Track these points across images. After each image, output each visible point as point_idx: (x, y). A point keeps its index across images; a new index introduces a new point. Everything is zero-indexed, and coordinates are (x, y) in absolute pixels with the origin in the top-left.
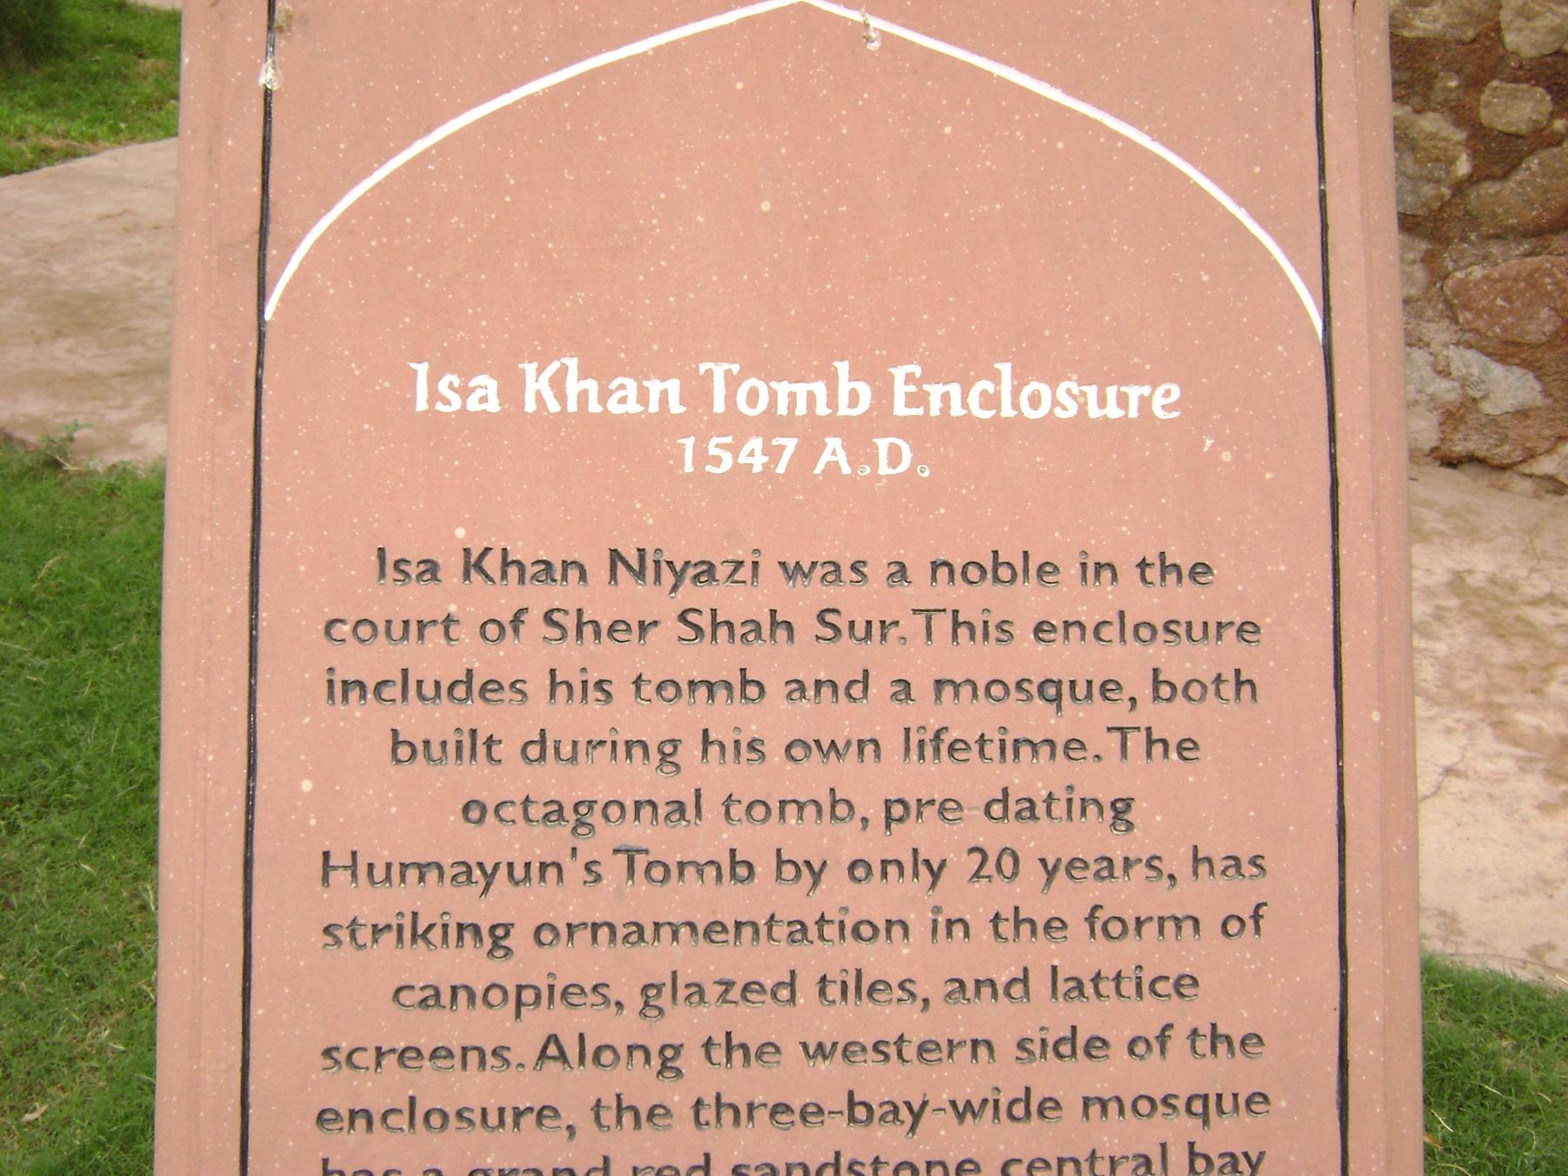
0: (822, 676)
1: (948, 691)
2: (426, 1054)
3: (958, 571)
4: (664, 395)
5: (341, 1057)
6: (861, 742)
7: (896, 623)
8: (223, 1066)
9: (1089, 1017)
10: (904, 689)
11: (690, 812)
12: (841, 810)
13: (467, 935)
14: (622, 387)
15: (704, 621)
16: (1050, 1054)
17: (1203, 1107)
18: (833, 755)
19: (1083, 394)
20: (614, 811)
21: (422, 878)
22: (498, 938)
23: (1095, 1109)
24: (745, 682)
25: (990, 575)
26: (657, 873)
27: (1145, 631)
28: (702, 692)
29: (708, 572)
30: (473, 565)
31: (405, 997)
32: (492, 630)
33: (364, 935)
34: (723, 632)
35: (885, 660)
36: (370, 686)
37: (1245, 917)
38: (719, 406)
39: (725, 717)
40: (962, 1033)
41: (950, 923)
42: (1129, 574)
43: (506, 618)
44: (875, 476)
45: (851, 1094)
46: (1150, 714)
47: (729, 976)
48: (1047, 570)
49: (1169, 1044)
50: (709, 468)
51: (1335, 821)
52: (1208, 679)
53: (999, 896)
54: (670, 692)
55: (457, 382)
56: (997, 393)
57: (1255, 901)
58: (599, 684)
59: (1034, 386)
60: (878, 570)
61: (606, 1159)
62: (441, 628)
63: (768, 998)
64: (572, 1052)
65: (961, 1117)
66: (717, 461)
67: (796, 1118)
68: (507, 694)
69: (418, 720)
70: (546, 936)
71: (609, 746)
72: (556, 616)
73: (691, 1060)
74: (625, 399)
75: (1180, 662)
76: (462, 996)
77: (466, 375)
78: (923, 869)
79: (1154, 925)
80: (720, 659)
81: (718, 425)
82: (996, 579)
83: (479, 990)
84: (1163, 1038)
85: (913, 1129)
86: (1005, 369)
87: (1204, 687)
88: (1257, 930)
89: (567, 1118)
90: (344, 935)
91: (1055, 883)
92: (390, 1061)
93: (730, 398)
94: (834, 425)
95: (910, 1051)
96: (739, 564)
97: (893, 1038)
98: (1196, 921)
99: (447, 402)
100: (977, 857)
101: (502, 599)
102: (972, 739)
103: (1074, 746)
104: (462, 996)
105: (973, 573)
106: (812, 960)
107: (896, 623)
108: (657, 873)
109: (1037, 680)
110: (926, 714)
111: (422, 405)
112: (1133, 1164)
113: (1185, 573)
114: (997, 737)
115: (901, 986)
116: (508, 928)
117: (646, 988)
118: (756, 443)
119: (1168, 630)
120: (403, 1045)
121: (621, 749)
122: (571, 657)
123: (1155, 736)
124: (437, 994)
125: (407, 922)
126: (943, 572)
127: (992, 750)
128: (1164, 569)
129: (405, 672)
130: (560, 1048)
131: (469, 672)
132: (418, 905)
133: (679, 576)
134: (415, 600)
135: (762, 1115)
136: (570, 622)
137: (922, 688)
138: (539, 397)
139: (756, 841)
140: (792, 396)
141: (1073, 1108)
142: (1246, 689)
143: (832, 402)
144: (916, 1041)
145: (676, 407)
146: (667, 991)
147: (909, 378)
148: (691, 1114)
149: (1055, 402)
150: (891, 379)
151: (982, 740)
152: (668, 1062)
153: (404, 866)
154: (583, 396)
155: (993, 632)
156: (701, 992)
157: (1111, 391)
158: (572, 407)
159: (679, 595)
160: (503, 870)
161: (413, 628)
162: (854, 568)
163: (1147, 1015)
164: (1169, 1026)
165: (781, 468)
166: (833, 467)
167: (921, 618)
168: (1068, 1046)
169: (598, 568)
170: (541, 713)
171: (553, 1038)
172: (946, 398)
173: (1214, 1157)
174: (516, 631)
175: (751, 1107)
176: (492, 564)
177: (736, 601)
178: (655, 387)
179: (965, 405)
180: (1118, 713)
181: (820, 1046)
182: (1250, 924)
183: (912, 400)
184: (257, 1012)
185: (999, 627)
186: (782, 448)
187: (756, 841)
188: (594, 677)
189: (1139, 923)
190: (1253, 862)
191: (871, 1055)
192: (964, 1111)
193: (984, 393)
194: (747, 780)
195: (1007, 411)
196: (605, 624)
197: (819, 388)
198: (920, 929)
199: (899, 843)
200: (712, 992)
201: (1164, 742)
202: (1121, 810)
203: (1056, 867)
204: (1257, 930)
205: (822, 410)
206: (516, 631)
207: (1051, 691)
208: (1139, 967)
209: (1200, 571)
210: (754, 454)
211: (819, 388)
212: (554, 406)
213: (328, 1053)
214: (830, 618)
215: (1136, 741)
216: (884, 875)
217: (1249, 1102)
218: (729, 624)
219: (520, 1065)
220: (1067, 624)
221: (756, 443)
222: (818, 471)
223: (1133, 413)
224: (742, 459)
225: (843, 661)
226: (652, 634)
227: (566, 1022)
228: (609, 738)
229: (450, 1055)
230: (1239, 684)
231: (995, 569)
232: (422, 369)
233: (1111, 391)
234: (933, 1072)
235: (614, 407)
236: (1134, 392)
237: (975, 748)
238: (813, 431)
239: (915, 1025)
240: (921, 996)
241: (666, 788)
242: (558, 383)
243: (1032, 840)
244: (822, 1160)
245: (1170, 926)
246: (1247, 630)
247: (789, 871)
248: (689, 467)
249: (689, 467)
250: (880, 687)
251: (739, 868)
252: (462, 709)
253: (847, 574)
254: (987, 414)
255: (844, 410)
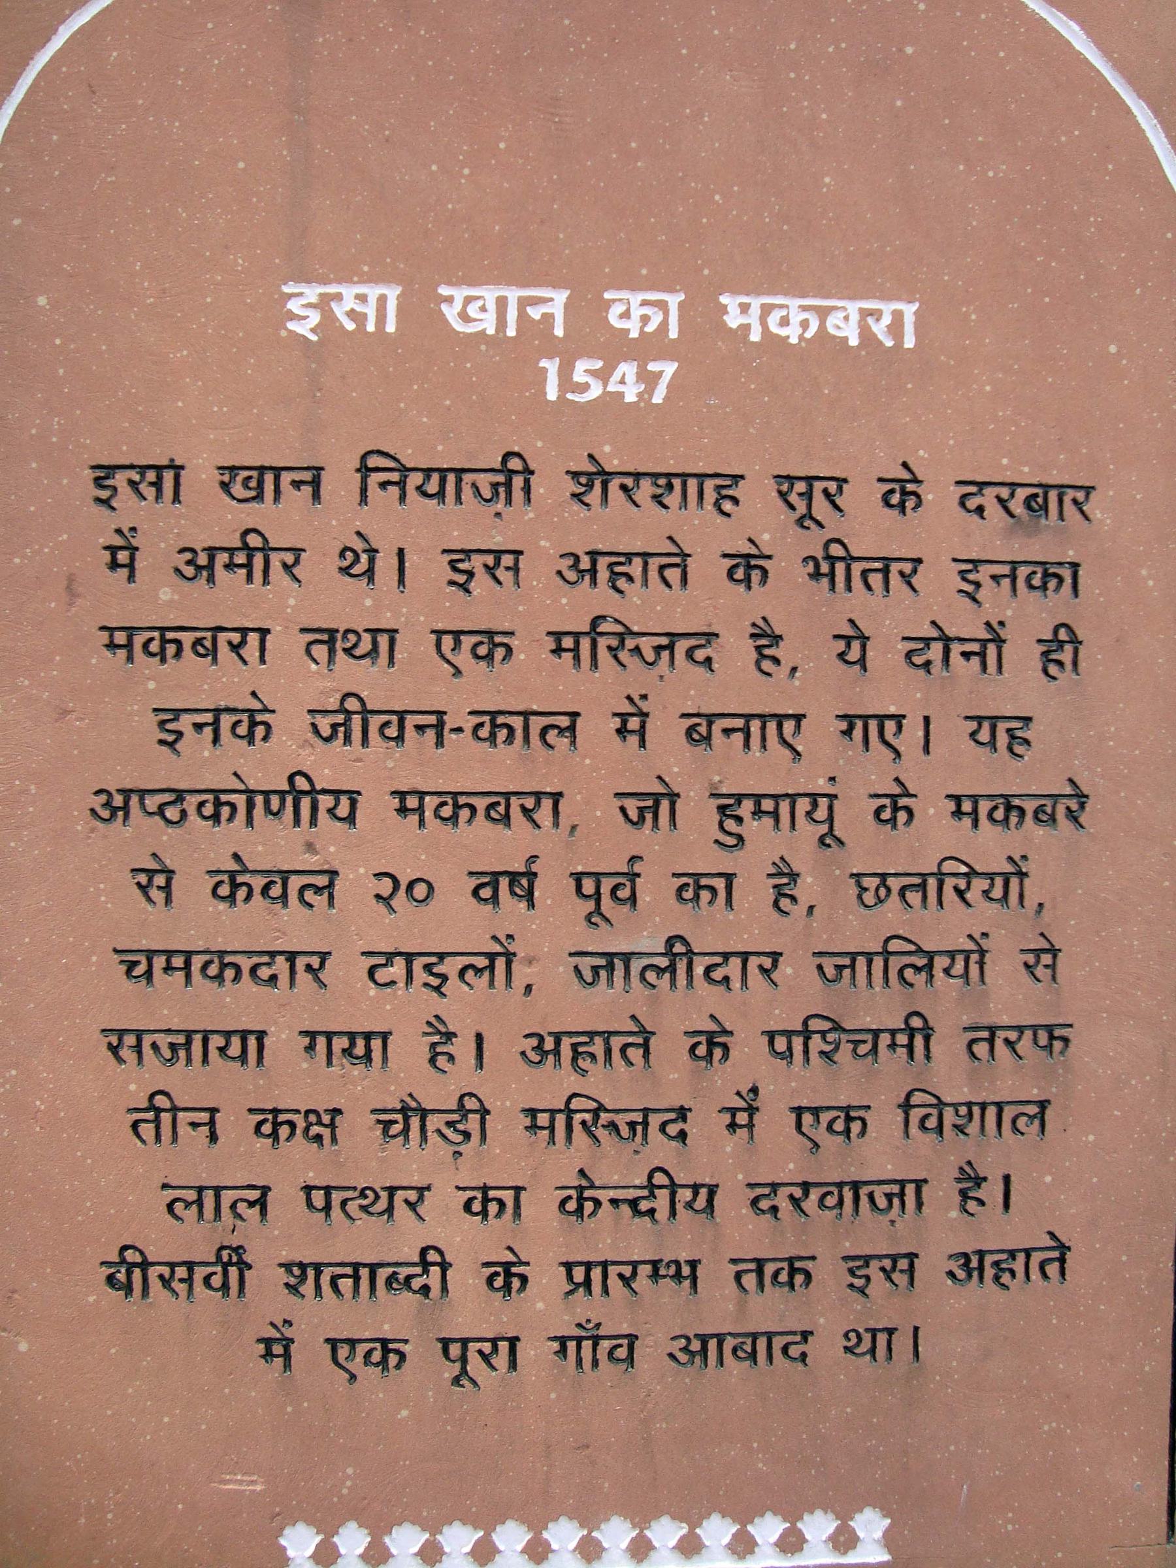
50: (570, 396)
66: (585, 387)
118: (628, 369)
165: (658, 398)
221: (628, 369)
224: (611, 388)
249: (552, 394)
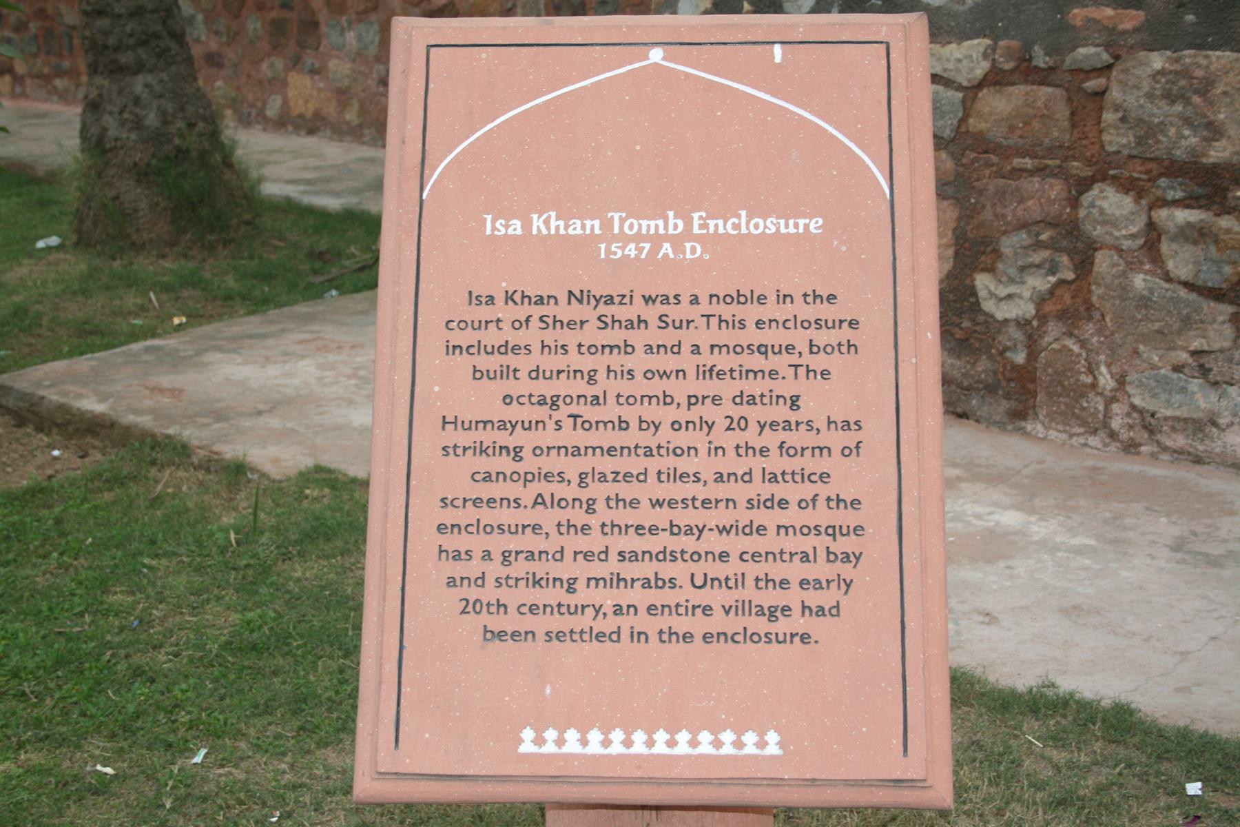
0: (660, 343)
1: (716, 350)
2: (485, 501)
3: (721, 298)
4: (593, 226)
5: (448, 502)
6: (678, 371)
7: (693, 321)
8: (398, 505)
9: (779, 490)
10: (696, 349)
11: (601, 401)
12: (668, 400)
13: (504, 451)
14: (574, 223)
15: (609, 320)
16: (762, 506)
17: (833, 531)
18: (664, 377)
19: (779, 223)
20: (568, 400)
21: (485, 428)
22: (517, 453)
23: (782, 531)
24: (626, 346)
25: (736, 300)
26: (587, 426)
27: (805, 325)
28: (607, 350)
29: (610, 300)
30: (509, 297)
31: (477, 477)
32: (517, 325)
33: (460, 451)
34: (617, 324)
35: (688, 337)
36: (464, 348)
37: (852, 447)
38: (616, 230)
39: (616, 360)
40: (721, 496)
41: (716, 448)
42: (799, 299)
43: (523, 319)
44: (685, 259)
45: (671, 521)
46: (807, 359)
47: (617, 470)
48: (762, 299)
49: (817, 503)
51: (894, 406)
52: (835, 344)
53: (738, 437)
54: (593, 350)
55: (503, 222)
56: (740, 224)
57: (857, 440)
58: (563, 347)
59: (756, 220)
60: (685, 299)
61: (562, 547)
62: (494, 324)
63: (634, 479)
64: (548, 501)
65: (721, 532)
66: (615, 253)
67: (646, 531)
68: (523, 351)
69: (484, 362)
70: (538, 452)
71: (566, 372)
72: (544, 319)
73: (600, 506)
74: (576, 228)
75: (823, 337)
76: (501, 477)
77: (508, 220)
78: (705, 426)
79: (810, 451)
80: (615, 336)
81: (616, 238)
82: (739, 302)
83: (508, 474)
84: (814, 500)
85: (698, 539)
86: (743, 213)
87: (833, 348)
88: (858, 454)
89: (545, 530)
90: (451, 451)
91: (764, 432)
92: (469, 504)
93: (621, 227)
94: (667, 238)
95: (698, 504)
96: (624, 296)
97: (690, 497)
98: (829, 449)
99: (499, 231)
100: (729, 420)
101: (521, 312)
102: (727, 369)
103: (773, 374)
104: (501, 477)
105: (728, 300)
106: (654, 464)
107: (693, 321)
108: (587, 426)
109: (756, 344)
110: (707, 359)
111: (488, 232)
112: (801, 556)
113: (825, 299)
114: (738, 369)
115: (694, 475)
116: (521, 448)
117: (581, 474)
118: (632, 246)
119: (816, 323)
120: (475, 497)
121: (572, 374)
122: (550, 336)
123: (810, 368)
124: (490, 476)
125: (478, 445)
126: (715, 299)
127: (736, 375)
128: (815, 297)
129: (479, 341)
130: (543, 499)
131: (507, 342)
132: (483, 438)
133: (598, 301)
134: (484, 312)
135: (632, 530)
136: (550, 321)
137: (705, 349)
138: (539, 229)
139: (631, 414)
140: (649, 226)
141: (772, 531)
142: (852, 349)
143: (666, 228)
144: (701, 498)
145: (597, 231)
146: (590, 476)
147: (700, 218)
148: (600, 529)
149: (766, 227)
150: (692, 218)
151: (732, 371)
152: (590, 508)
153: (477, 422)
154: (558, 227)
155: (737, 324)
156: (605, 476)
157: (791, 222)
158: (553, 232)
159: (598, 309)
160: (520, 424)
161: (483, 324)
162: (676, 297)
163: (807, 491)
164: (817, 495)
165: (643, 256)
166: (666, 255)
167: (705, 318)
168: (770, 503)
169: (563, 298)
170: (536, 359)
171: (540, 495)
172: (716, 226)
173: (838, 553)
174: (527, 325)
175: (627, 527)
176: (517, 297)
177: (623, 313)
178: (588, 223)
179: (725, 228)
180: (795, 359)
181: (658, 500)
182: (854, 451)
183: (701, 227)
184: (413, 483)
185: (740, 322)
186: (644, 248)
187: (631, 414)
188: (560, 343)
189: (803, 449)
190: (856, 423)
191: (680, 505)
192: (723, 530)
193: (733, 223)
194: (625, 387)
195: (744, 231)
196: (565, 322)
197: (661, 223)
198: (703, 451)
199: (694, 414)
200: (610, 477)
201: (815, 371)
202: (794, 402)
203: (765, 424)
204: (858, 454)
205: (662, 231)
206: (527, 325)
207: (763, 349)
208: (803, 469)
209: (831, 298)
210: (631, 251)
211: (661, 223)
212: (545, 232)
213: (443, 500)
214: (664, 318)
215: (802, 371)
216: (687, 428)
217: (855, 529)
218: (620, 322)
219: (525, 507)
220: (770, 321)
221: (632, 246)
222: (659, 257)
223: (801, 230)
224: (626, 253)
225: (670, 337)
226: (585, 326)
227: (546, 489)
228: (566, 369)
229: (495, 501)
230: (849, 346)
231: (739, 298)
232: (489, 218)
233: (791, 222)
234: (708, 512)
235: (571, 231)
236: (801, 222)
237: (729, 373)
238: (657, 240)
239: (700, 492)
240: (703, 480)
241: (590, 391)
242: (547, 222)
243: (753, 414)
244: (658, 550)
245: (817, 451)
246: (853, 324)
247: (644, 426)
248: (603, 256)
249: (603, 256)
250: (687, 348)
251: (623, 425)
252: (503, 357)
253: (672, 300)
254: (735, 232)
255: (671, 231)
